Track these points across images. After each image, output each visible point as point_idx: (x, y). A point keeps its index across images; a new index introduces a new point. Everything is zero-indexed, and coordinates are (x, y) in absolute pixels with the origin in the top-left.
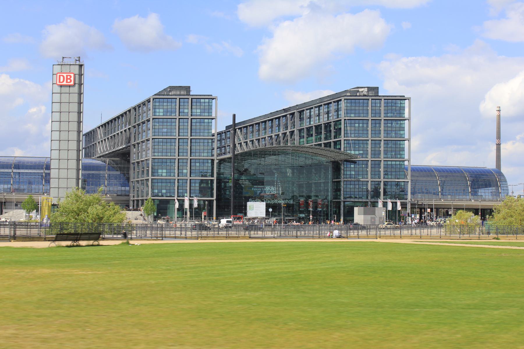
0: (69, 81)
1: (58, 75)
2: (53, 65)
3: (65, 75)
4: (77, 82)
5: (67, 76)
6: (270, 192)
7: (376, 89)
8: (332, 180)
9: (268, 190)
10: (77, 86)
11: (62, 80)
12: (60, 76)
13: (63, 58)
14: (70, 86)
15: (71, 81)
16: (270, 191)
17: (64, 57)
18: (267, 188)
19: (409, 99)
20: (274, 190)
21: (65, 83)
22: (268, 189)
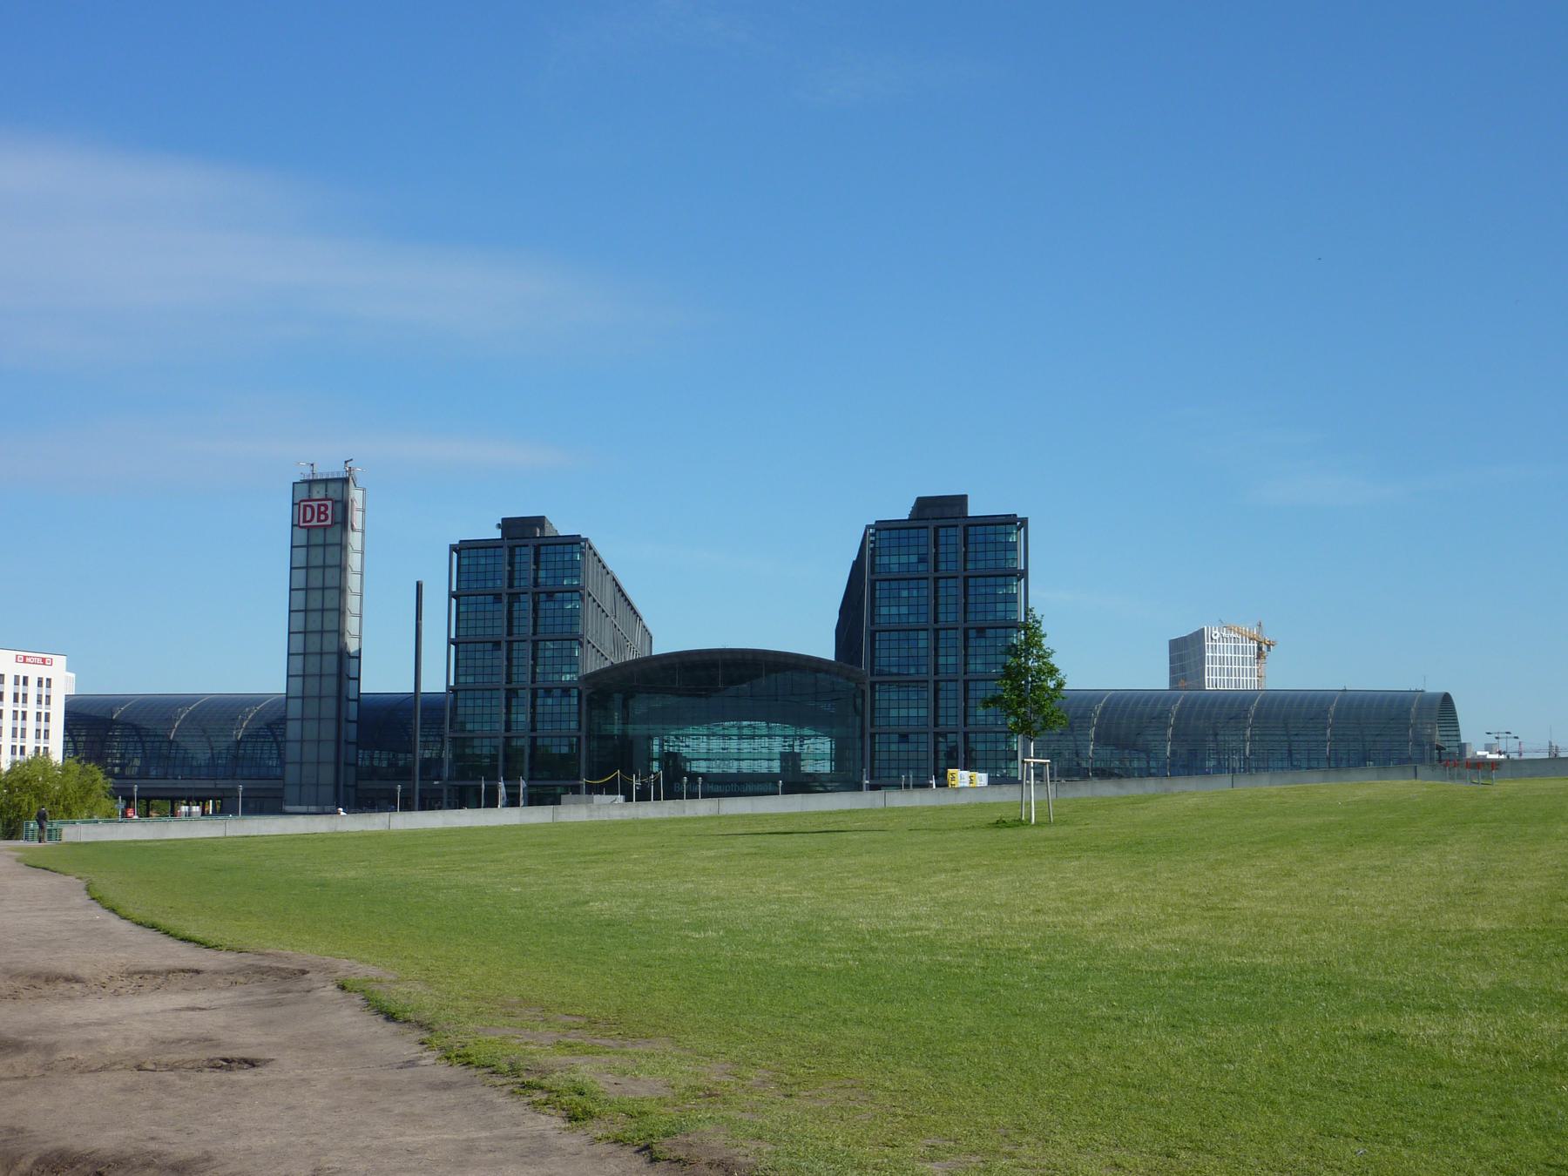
0: (323, 517)
1: (302, 504)
2: (294, 483)
3: (315, 504)
4: (339, 518)
5: (319, 506)
7: (961, 500)
10: (338, 527)
11: (308, 519)
12: (305, 506)
14: (325, 527)
15: (326, 519)
21: (315, 523)
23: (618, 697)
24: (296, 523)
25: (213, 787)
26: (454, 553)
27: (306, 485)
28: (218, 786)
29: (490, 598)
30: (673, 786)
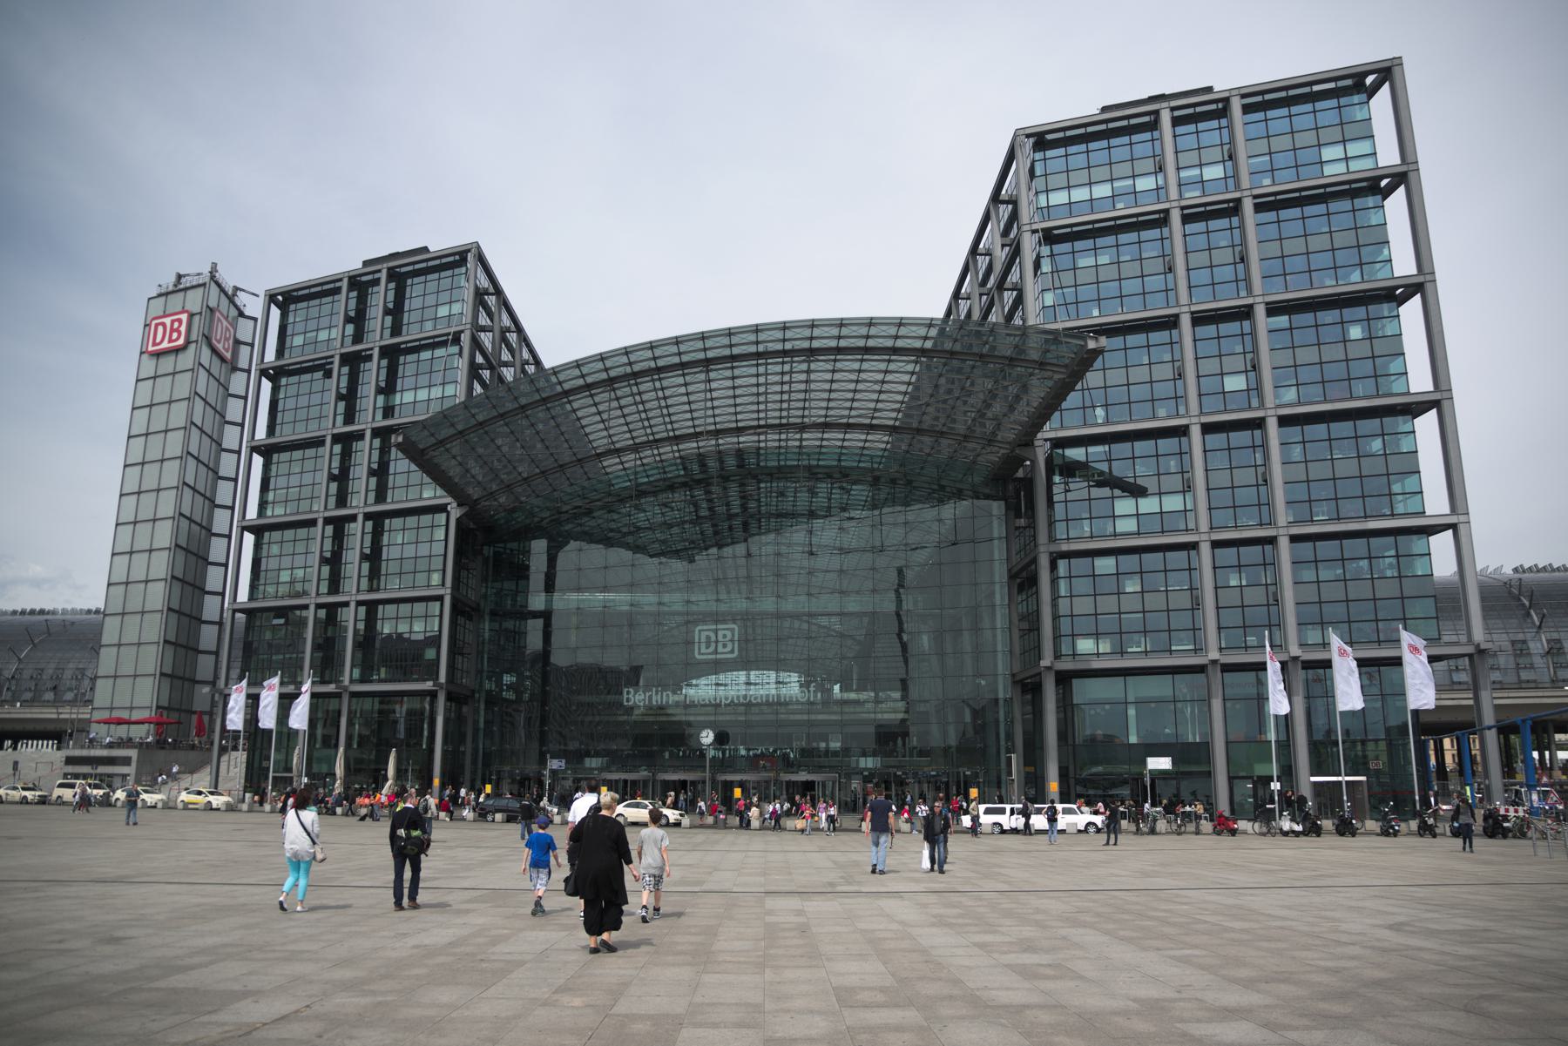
0: (175, 335)
2: (150, 299)
3: (168, 321)
5: (173, 322)
6: (711, 649)
8: (1009, 570)
9: (703, 639)
11: (158, 339)
12: (157, 325)
13: (180, 277)
14: (177, 351)
16: (713, 645)
17: (182, 273)
18: (700, 631)
19: (1387, 72)
20: (732, 641)
21: (165, 345)
22: (704, 635)
23: (539, 546)
24: (144, 350)
25: (55, 716)
26: (273, 307)
27: (163, 298)
28: (62, 716)
29: (319, 374)
30: (621, 693)
